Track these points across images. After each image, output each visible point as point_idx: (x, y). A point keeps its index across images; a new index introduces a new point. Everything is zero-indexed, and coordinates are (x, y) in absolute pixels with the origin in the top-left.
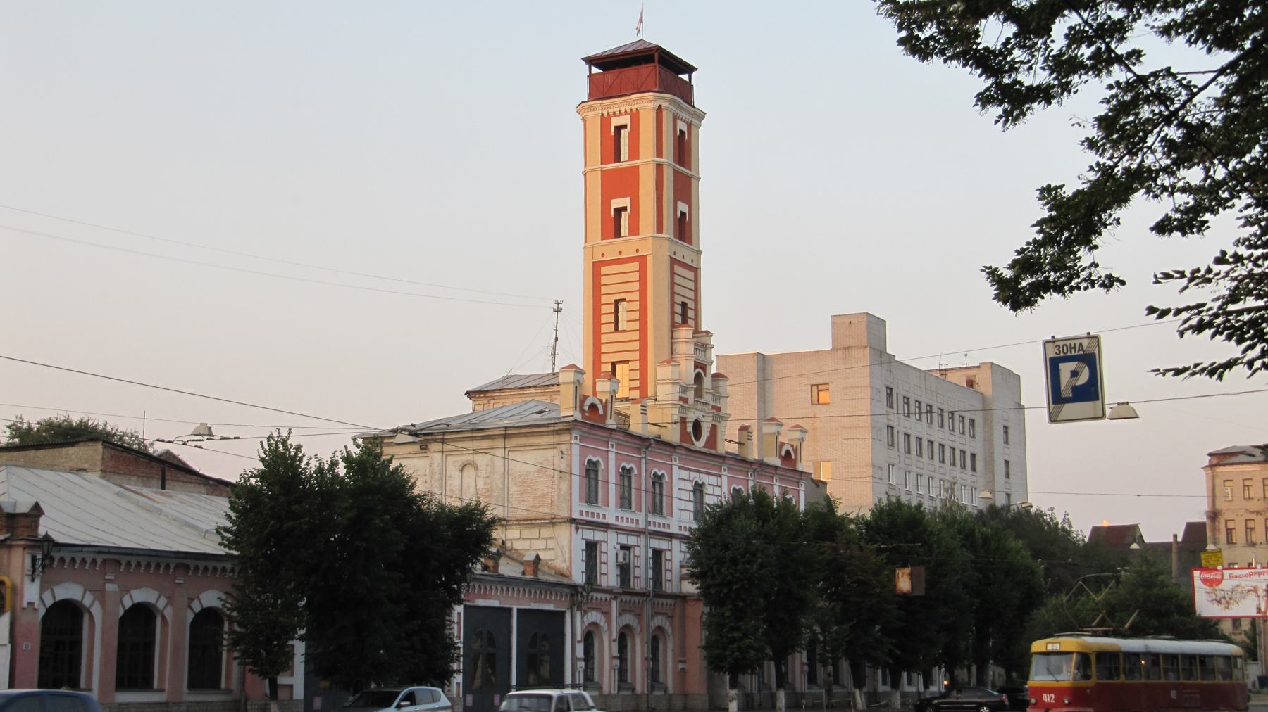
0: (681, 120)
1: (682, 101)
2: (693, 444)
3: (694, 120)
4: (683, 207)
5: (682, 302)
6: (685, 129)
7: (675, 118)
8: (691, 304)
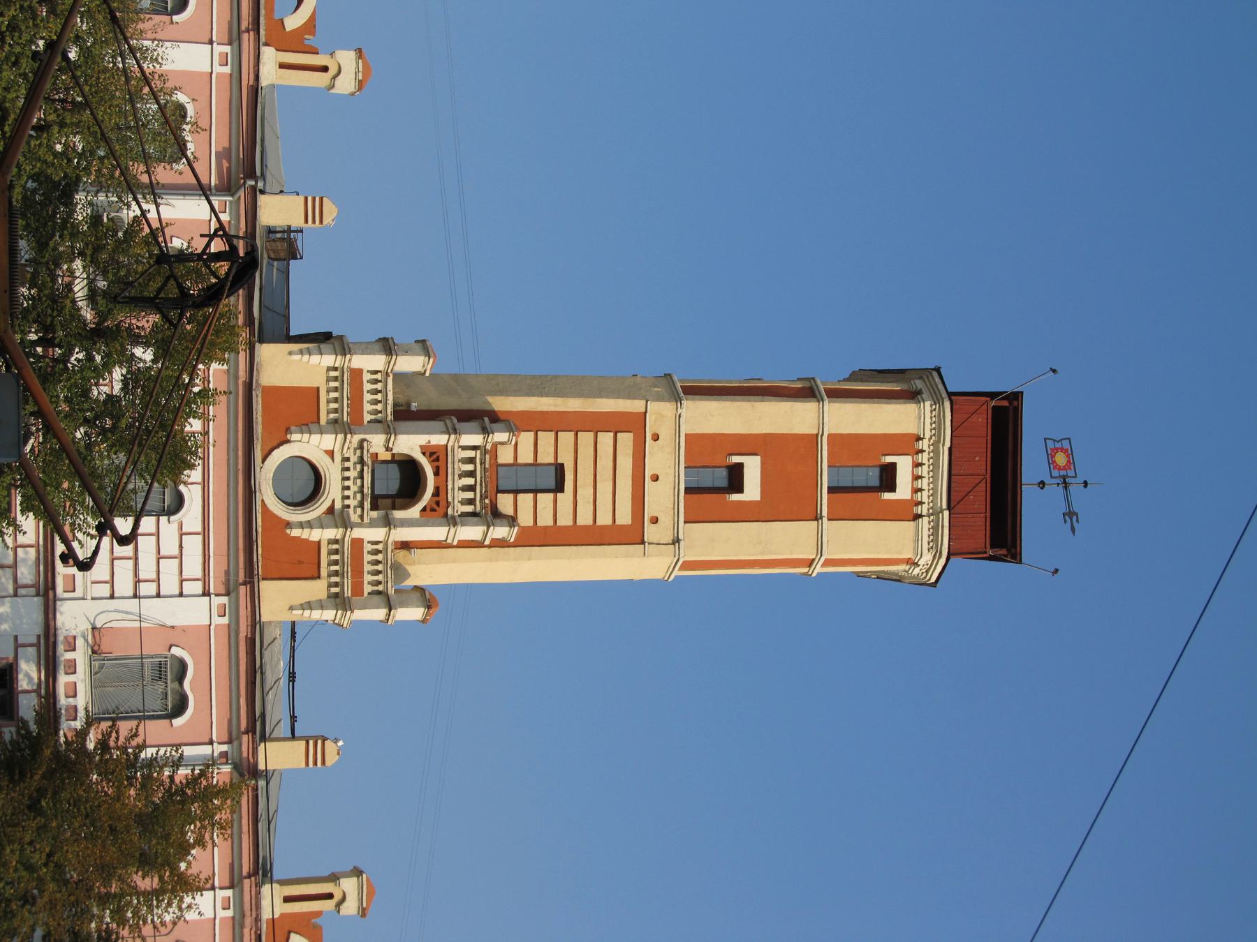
0: (917, 478)
1: (948, 444)
2: (263, 461)
3: (926, 520)
4: (752, 468)
5: (562, 465)
6: (903, 490)
7: (908, 444)
8: (565, 498)
